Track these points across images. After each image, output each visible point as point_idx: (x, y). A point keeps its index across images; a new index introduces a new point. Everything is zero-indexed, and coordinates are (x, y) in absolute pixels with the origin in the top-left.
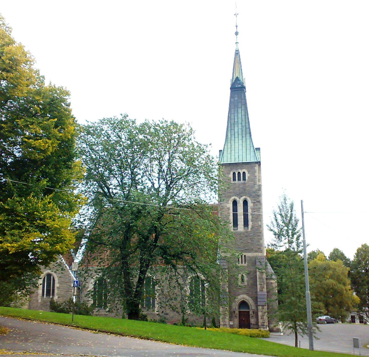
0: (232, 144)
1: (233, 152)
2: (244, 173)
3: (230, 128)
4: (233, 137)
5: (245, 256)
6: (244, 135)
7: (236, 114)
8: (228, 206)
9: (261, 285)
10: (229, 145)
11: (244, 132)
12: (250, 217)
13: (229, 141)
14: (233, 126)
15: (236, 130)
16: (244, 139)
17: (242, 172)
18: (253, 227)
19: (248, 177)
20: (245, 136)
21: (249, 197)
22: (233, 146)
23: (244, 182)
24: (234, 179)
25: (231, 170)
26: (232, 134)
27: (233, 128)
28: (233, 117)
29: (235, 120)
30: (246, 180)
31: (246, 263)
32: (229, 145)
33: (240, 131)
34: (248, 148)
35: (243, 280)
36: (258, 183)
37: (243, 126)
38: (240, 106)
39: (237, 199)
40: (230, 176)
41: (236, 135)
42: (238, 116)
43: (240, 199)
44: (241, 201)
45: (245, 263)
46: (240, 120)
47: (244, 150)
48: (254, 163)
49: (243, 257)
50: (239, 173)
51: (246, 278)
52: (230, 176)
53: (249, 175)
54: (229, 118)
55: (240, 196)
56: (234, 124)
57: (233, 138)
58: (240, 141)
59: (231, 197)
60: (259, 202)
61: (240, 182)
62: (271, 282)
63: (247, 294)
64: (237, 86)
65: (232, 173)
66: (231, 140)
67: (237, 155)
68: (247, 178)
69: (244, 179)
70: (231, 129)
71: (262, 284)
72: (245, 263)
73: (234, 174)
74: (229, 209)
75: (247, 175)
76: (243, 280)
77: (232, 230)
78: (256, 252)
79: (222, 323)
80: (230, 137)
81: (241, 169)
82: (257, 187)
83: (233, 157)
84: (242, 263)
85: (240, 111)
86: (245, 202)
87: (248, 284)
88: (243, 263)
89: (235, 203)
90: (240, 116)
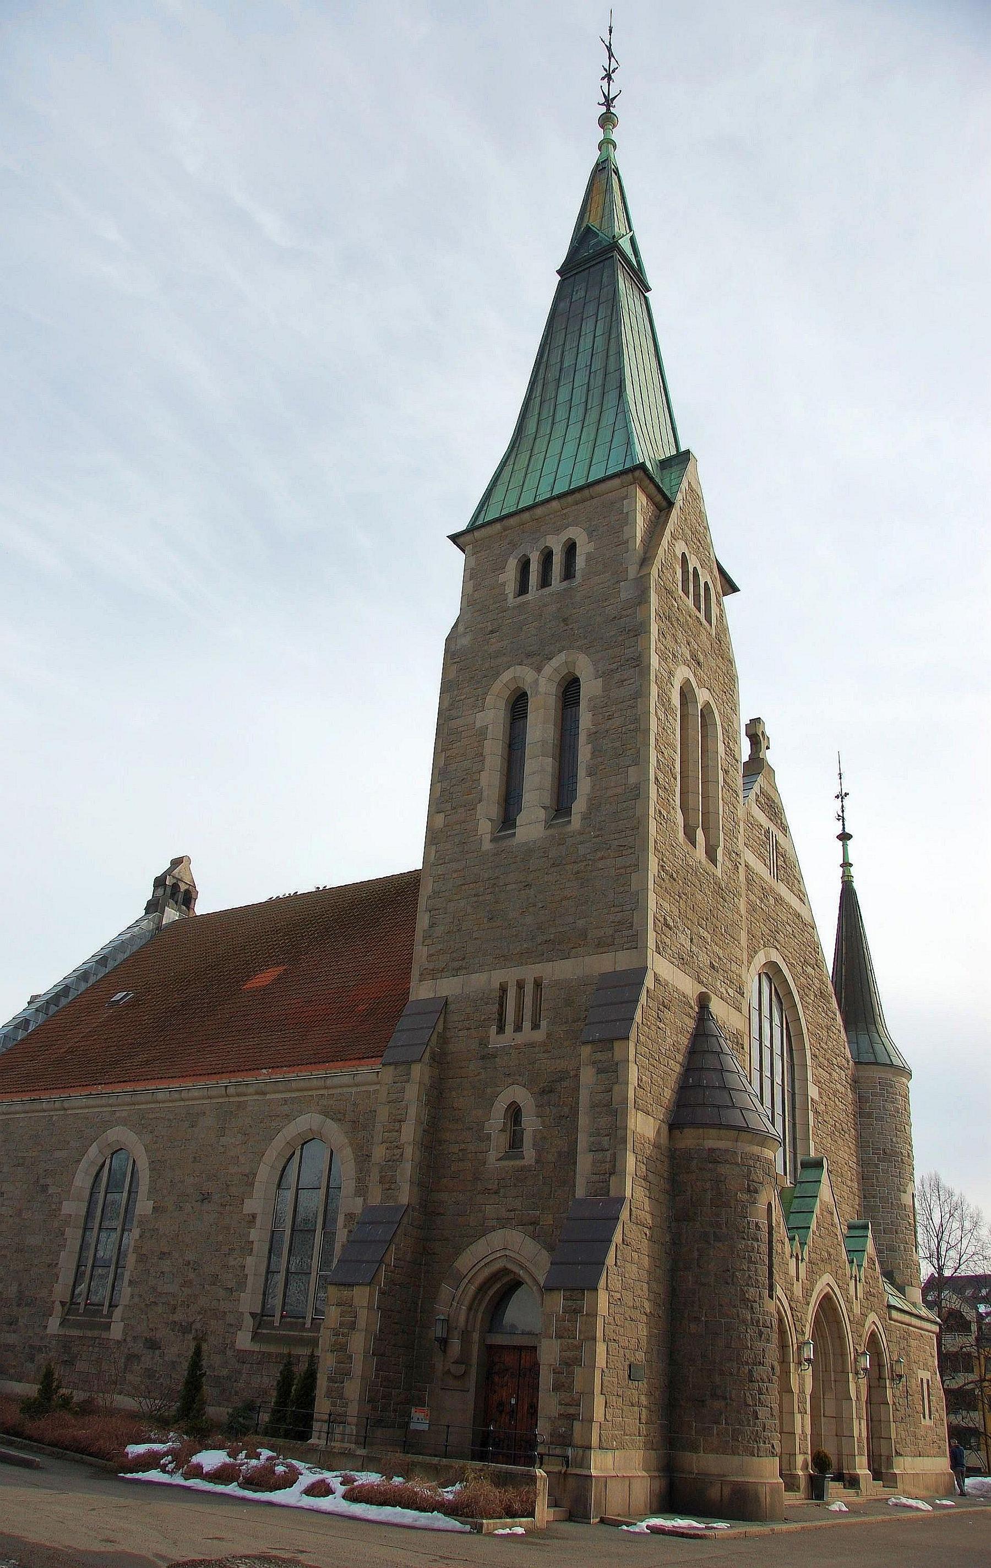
5: (538, 984)
6: (594, 402)
8: (478, 725)
9: (600, 1156)
12: (584, 753)
18: (594, 805)
19: (589, 557)
21: (585, 650)
23: (565, 584)
24: (523, 588)
25: (514, 545)
26: (544, 415)
30: (578, 574)
31: (543, 1024)
34: (605, 435)
36: (632, 572)
41: (561, 414)
44: (542, 681)
45: (536, 1026)
48: (616, 482)
49: (529, 989)
51: (530, 1123)
53: (590, 547)
55: (538, 658)
57: (545, 429)
59: (498, 674)
61: (547, 590)
62: (711, 1150)
63: (531, 1226)
68: (580, 562)
69: (569, 573)
72: (536, 1026)
74: (482, 733)
77: (487, 846)
78: (603, 945)
84: (518, 1028)
87: (537, 1162)
88: (527, 1025)
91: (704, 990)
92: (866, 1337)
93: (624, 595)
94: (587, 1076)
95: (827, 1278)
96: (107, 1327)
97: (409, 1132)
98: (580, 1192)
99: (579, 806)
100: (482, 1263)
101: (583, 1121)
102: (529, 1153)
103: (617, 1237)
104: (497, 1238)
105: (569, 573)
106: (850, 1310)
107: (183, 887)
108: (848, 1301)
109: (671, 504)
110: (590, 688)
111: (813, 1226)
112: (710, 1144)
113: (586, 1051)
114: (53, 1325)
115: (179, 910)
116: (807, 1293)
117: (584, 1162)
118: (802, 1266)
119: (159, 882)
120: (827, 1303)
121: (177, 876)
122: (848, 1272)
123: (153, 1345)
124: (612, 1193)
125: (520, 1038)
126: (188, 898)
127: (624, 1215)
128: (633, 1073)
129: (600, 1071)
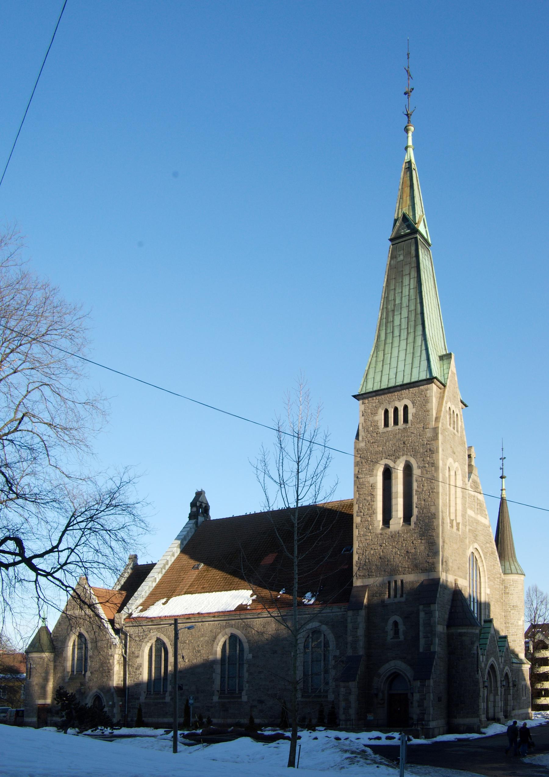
0: (386, 352)
1: (386, 367)
2: (406, 408)
3: (384, 320)
4: (390, 336)
6: (411, 330)
7: (398, 290)
10: (381, 354)
11: (412, 324)
13: (382, 347)
14: (391, 314)
15: (397, 322)
16: (411, 336)
17: (401, 406)
20: (412, 330)
21: (414, 456)
22: (388, 356)
23: (404, 426)
24: (386, 424)
26: (388, 331)
27: (391, 319)
28: (391, 297)
29: (397, 302)
30: (409, 422)
32: (381, 354)
33: (404, 322)
35: (396, 632)
37: (411, 311)
38: (406, 271)
39: (391, 464)
40: (376, 418)
42: (402, 292)
43: (395, 463)
46: (405, 303)
47: (409, 361)
50: (396, 410)
51: (401, 628)
52: (376, 418)
54: (386, 299)
56: (393, 311)
57: (389, 340)
58: (403, 343)
60: (434, 465)
61: (397, 427)
64: (402, 233)
65: (381, 413)
66: (385, 344)
67: (393, 371)
68: (410, 417)
69: (406, 420)
70: (387, 323)
71: (428, 637)
73: (386, 412)
75: (411, 411)
76: (396, 632)
79: (342, 717)
80: (384, 339)
81: (399, 400)
82: (429, 434)
83: (385, 379)
85: (406, 281)
86: (408, 469)
89: (388, 474)
90: (406, 291)
91: (456, 578)
92: (504, 674)
93: (429, 435)
94: (422, 615)
95: (492, 659)
96: (241, 697)
97: (361, 632)
98: (421, 650)
99: (413, 519)
100: (387, 671)
101: (421, 628)
102: (402, 637)
103: (434, 663)
104: (392, 663)
105: (406, 420)
106: (499, 668)
107: (204, 505)
108: (499, 665)
109: (444, 386)
110: (416, 472)
111: (488, 643)
112: (460, 631)
113: (421, 607)
114: (216, 698)
115: (204, 516)
116: (486, 665)
117: (422, 641)
118: (484, 657)
119: (193, 504)
120: (492, 667)
121: (201, 501)
122: (499, 655)
123: (261, 702)
124: (432, 650)
125: (396, 600)
126: (206, 509)
127: (436, 656)
128: (437, 614)
129: (426, 613)
